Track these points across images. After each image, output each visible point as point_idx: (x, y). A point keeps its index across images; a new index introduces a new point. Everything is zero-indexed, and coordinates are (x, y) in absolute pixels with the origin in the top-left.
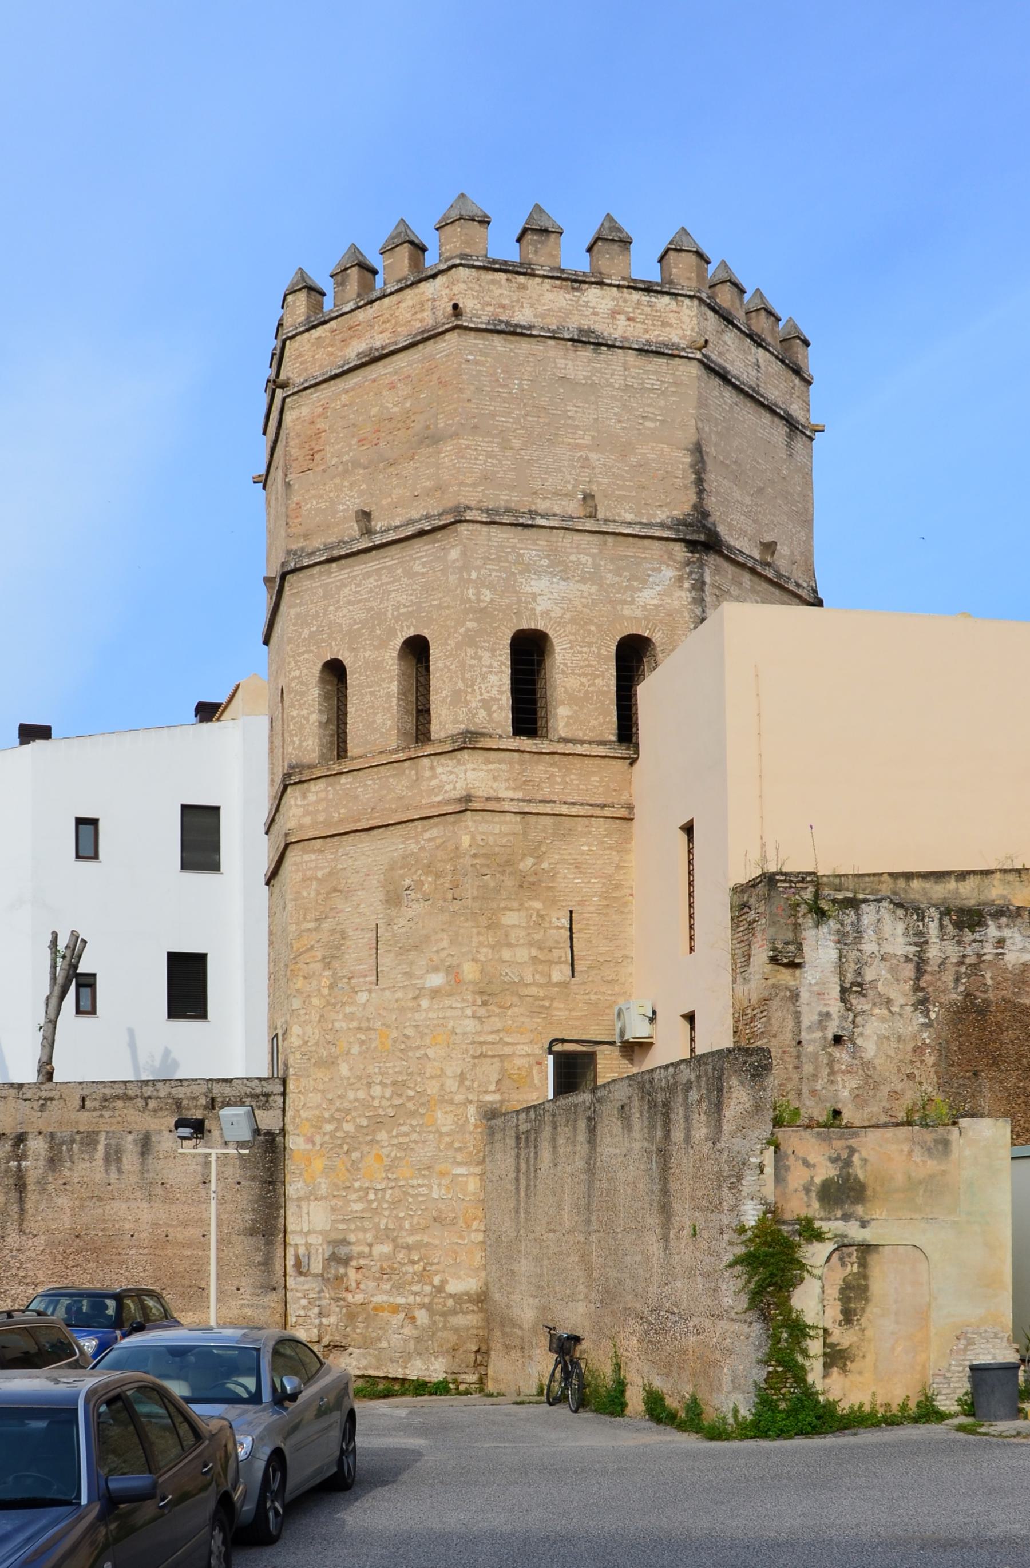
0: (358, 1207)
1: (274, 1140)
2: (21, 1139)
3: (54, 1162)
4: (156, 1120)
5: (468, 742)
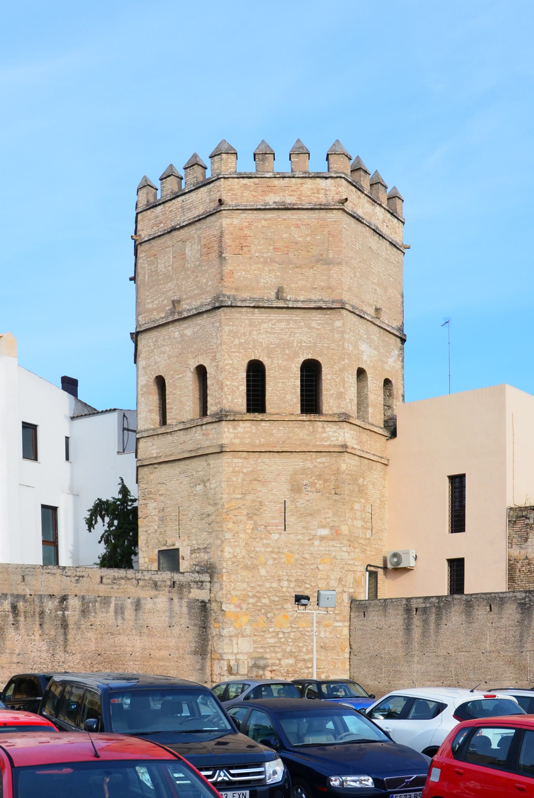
0: (272, 641)
1: (205, 605)
2: (64, 598)
3: (84, 612)
4: (143, 592)
5: (344, 419)
